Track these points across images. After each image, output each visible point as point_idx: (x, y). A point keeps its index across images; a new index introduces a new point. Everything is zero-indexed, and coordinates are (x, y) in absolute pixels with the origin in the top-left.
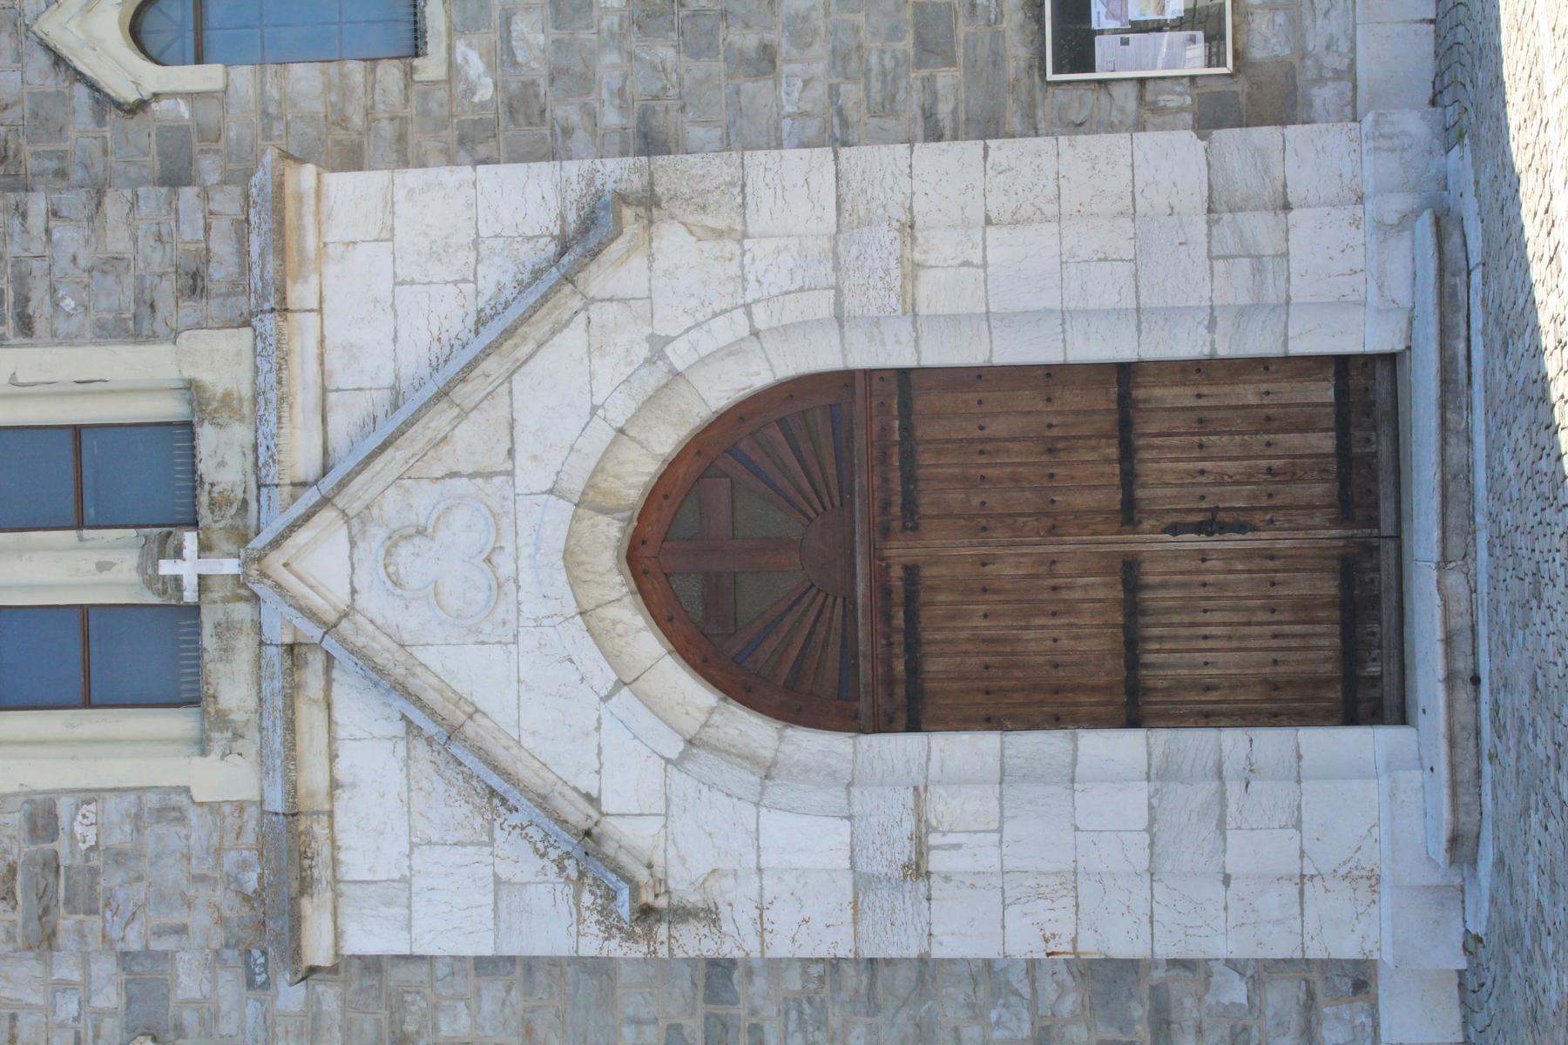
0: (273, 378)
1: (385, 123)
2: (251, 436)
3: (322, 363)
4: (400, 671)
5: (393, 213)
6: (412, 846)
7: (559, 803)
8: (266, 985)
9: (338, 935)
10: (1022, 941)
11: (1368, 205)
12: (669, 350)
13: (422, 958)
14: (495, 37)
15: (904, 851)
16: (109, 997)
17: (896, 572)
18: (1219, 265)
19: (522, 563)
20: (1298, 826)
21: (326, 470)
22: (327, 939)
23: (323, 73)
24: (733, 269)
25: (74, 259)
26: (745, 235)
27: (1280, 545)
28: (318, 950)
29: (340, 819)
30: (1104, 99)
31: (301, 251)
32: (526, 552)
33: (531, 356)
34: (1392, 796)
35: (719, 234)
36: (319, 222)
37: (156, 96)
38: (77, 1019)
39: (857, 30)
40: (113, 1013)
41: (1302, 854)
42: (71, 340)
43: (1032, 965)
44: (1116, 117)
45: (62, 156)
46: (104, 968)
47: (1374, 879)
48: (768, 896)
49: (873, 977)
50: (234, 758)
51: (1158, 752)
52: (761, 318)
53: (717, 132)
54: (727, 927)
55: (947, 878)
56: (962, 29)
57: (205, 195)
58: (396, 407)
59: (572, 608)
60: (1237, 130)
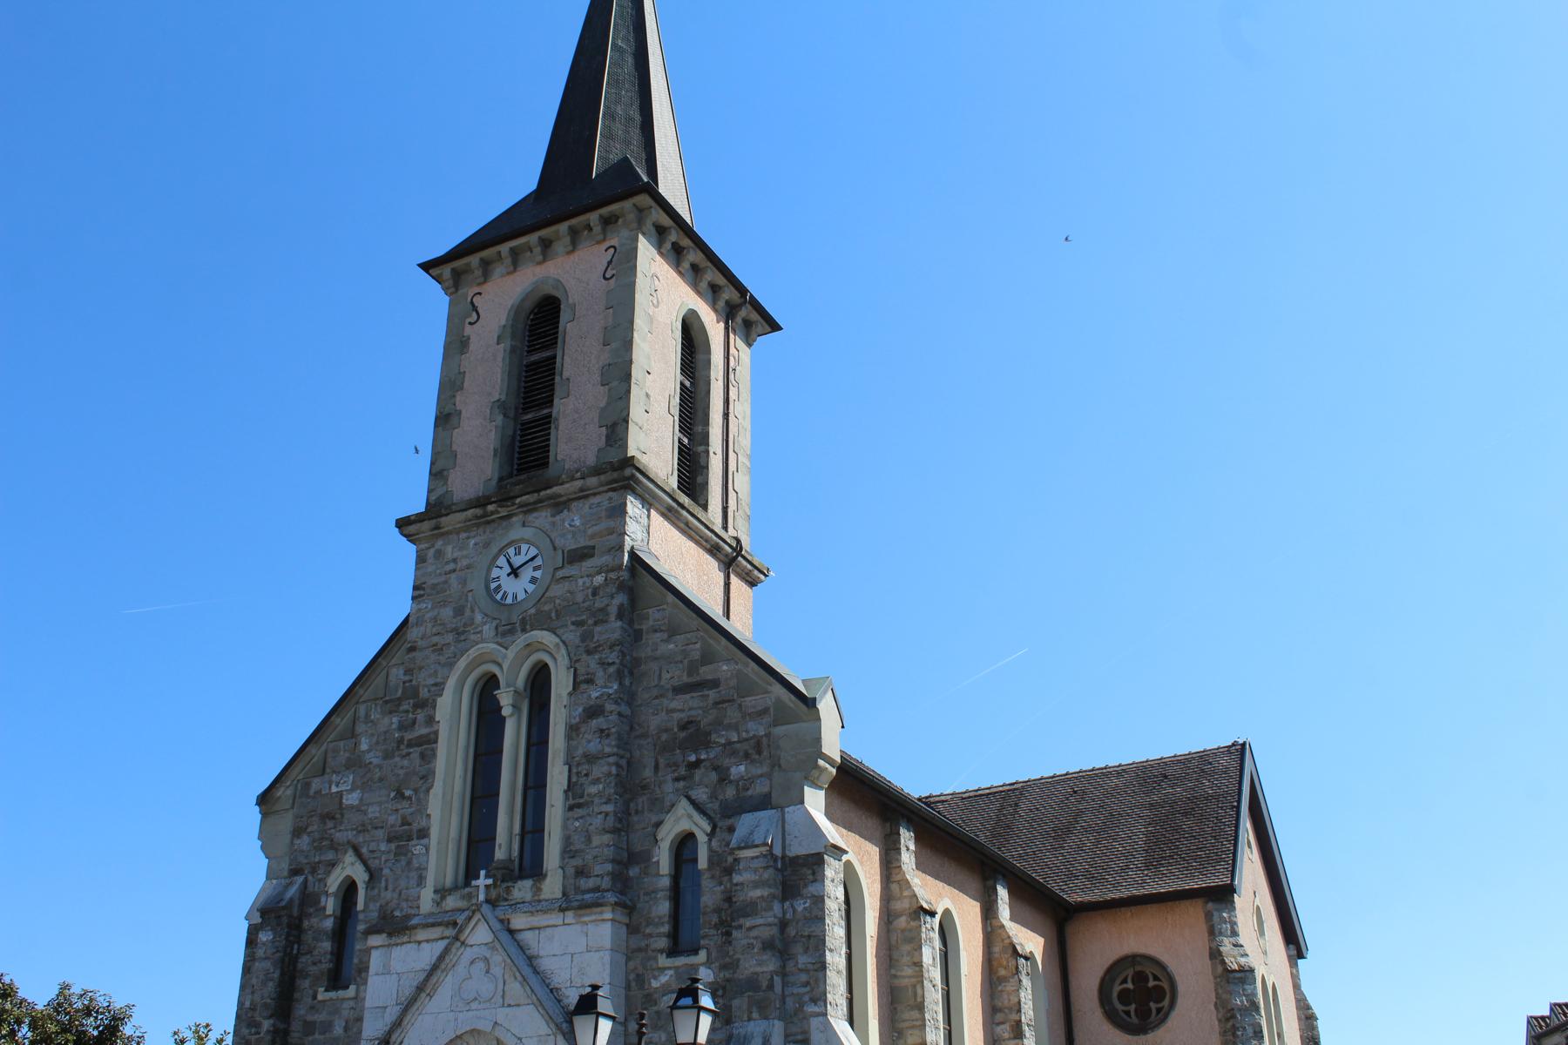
3: (548, 926)
4: (443, 966)
5: (596, 951)
6: (399, 974)
7: (399, 1031)
9: (377, 947)
19: (475, 1012)
23: (665, 915)
25: (591, 824)
29: (409, 945)
32: (478, 1013)
33: (540, 1013)
42: (565, 827)
45: (643, 812)
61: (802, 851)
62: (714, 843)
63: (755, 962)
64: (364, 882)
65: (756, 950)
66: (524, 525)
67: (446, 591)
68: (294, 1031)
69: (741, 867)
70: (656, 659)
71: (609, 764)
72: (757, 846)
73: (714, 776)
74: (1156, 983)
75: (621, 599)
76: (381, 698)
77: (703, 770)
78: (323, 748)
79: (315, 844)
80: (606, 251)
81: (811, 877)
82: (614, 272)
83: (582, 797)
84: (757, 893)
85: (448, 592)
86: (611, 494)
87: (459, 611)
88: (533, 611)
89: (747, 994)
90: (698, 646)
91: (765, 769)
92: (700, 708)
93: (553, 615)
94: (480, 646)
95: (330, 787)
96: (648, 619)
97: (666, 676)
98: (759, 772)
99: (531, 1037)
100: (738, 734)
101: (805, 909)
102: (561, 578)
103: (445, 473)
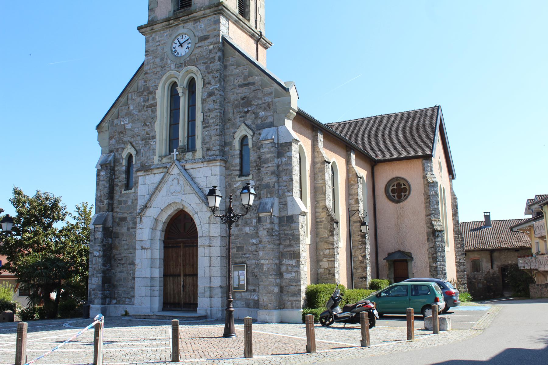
2: (191, 159)
4: (163, 182)
9: (140, 176)
15: (144, 247)
18: (203, 288)
20: (146, 296)
22: (140, 175)
24: (205, 223)
32: (176, 196)
34: (148, 308)
36: (214, 166)
42: (202, 134)
45: (229, 128)
51: (156, 278)
56: (240, 253)
61: (284, 141)
65: (269, 175)
66: (183, 28)
69: (263, 147)
70: (232, 75)
71: (217, 112)
72: (269, 140)
73: (253, 116)
74: (404, 186)
75: (219, 54)
77: (250, 114)
78: (118, 109)
81: (287, 150)
83: (208, 124)
84: (269, 155)
86: (214, 16)
87: (162, 60)
88: (188, 59)
89: (266, 189)
90: (247, 70)
91: (271, 113)
92: (248, 92)
93: (195, 60)
94: (169, 72)
96: (229, 61)
97: (236, 81)
98: (269, 114)
102: (198, 47)
103: (154, 9)
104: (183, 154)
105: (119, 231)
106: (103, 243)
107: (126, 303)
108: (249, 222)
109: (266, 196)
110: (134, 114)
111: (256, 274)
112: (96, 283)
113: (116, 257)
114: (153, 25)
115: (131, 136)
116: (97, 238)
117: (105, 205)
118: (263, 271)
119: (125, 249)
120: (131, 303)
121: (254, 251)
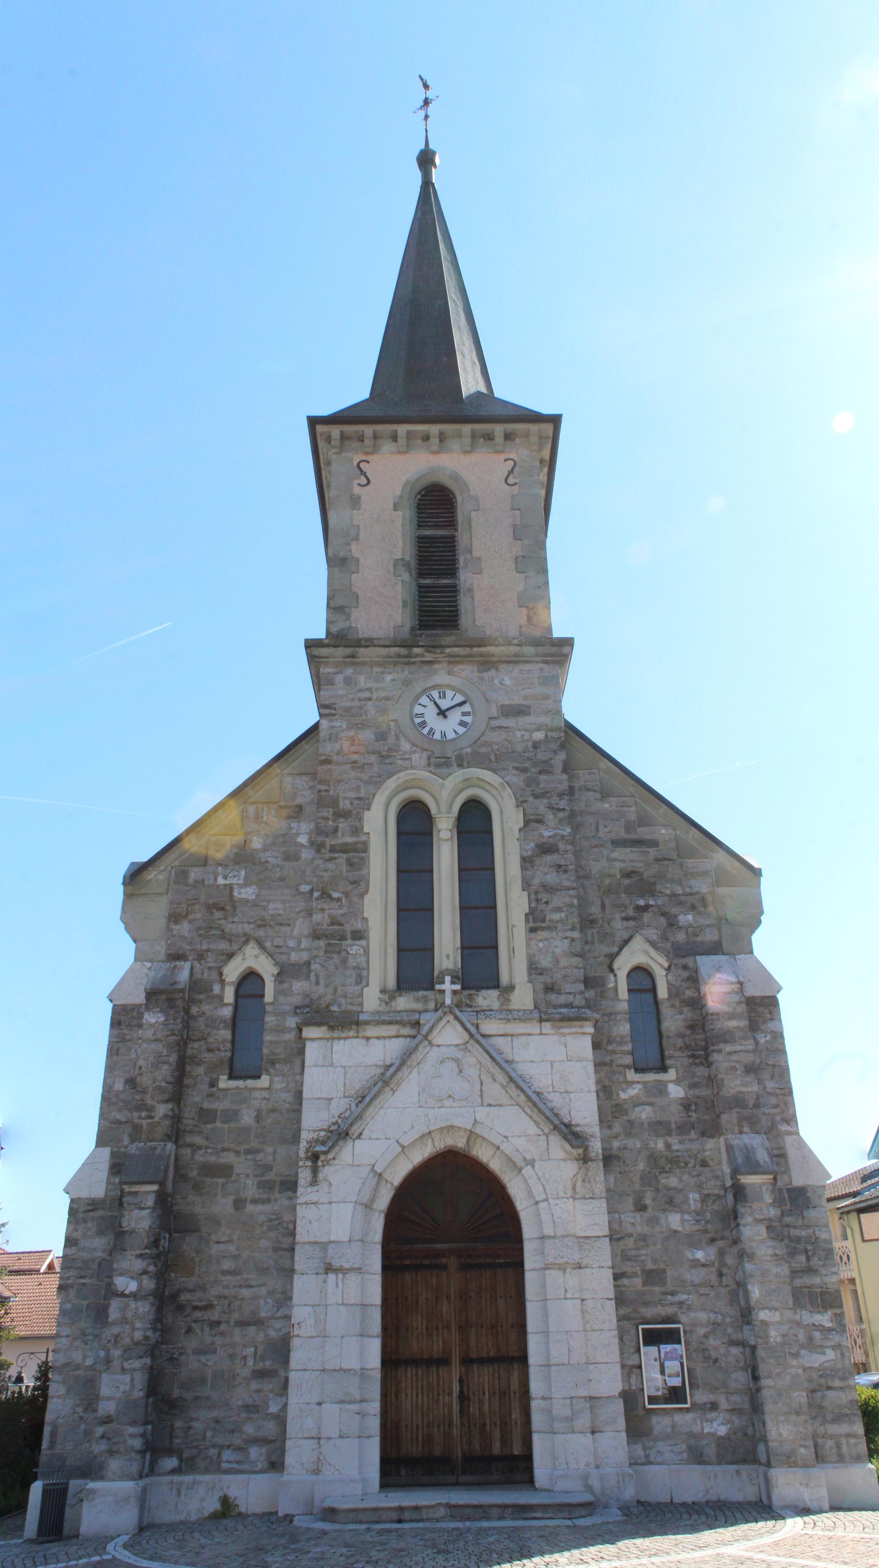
0: (516, 1016)
1: (609, 1058)
3: (522, 1034)
4: (409, 1063)
6: (345, 1067)
7: (359, 1123)
8: (296, 1013)
9: (313, 1040)
10: (299, 1313)
11: (595, 1471)
12: (529, 1167)
13: (303, 1070)
14: (644, 1099)
15: (336, 1263)
16: (294, 957)
17: (444, 1261)
18: (568, 1402)
19: (449, 1110)
20: (341, 1437)
21: (483, 1036)
23: (627, 1036)
24: (561, 1194)
26: (574, 1199)
27: (455, 1429)
28: (308, 1032)
30: (632, 1350)
31: (563, 1027)
32: (453, 1110)
33: (526, 1113)
34: (352, 1481)
35: (574, 1188)
36: (573, 1034)
37: (615, 976)
38: (287, 947)
39: (654, 1245)
40: (289, 959)
41: (329, 1438)
42: (528, 946)
43: (288, 1317)
44: (626, 1355)
45: (593, 943)
46: (305, 956)
47: (317, 1472)
48: (320, 1206)
49: (286, 1250)
50: (379, 1002)
52: (543, 1205)
53: (612, 1187)
54: (310, 1189)
55: (325, 1281)
56: (657, 1289)
57: (581, 993)
58: (507, 1062)
59: (432, 1128)
60: (623, 1410)
61: (757, 993)
62: (670, 977)
63: (739, 1082)
64: (273, 975)
65: (738, 1072)
66: (449, 674)
67: (361, 716)
68: (186, 1118)
70: (592, 814)
71: (570, 896)
73: (663, 921)
75: (562, 756)
76: (275, 803)
77: (651, 914)
79: (202, 932)
80: (505, 460)
81: (768, 1016)
82: (517, 481)
83: (544, 921)
84: (734, 1023)
85: (364, 717)
86: (545, 666)
87: (382, 736)
88: (469, 750)
89: (734, 1110)
90: (633, 809)
92: (641, 861)
93: (493, 757)
95: (215, 879)
96: (579, 778)
97: (602, 829)
98: (707, 922)
99: (519, 1136)
100: (683, 888)
101: (766, 1041)
104: (467, 992)
105: (198, 1209)
106: (157, 1247)
107: (224, 1465)
108: (678, 1198)
109: (736, 1129)
110: (267, 862)
111: (714, 1354)
112: (118, 1395)
113: (184, 1297)
114: (359, 646)
115: (254, 922)
116: (132, 1232)
117: (156, 1119)
118: (767, 1343)
119: (224, 1273)
120: (246, 1467)
121: (700, 1285)
